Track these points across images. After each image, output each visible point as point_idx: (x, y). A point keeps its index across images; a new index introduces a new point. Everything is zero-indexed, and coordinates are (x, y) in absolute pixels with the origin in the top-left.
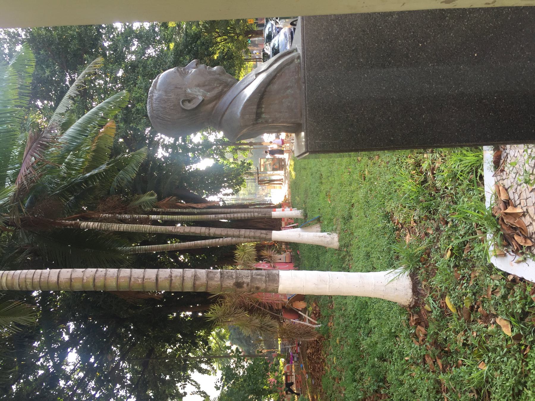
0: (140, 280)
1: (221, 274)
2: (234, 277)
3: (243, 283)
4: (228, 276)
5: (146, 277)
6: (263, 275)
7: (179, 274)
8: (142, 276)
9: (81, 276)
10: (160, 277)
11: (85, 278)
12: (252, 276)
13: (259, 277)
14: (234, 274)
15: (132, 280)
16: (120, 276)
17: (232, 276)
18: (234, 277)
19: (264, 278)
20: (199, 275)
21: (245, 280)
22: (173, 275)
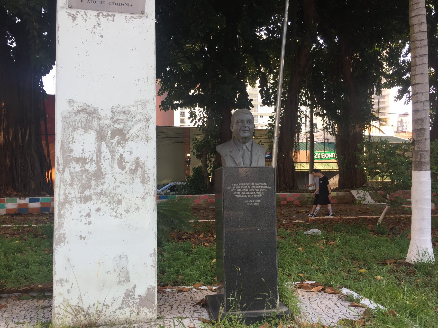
0: (414, 73)
1: (421, 129)
2: (418, 139)
3: (414, 146)
4: (419, 134)
5: (416, 76)
6: (420, 159)
7: (419, 99)
8: (416, 73)
9: (415, 32)
10: (417, 86)
11: (414, 35)
12: (419, 151)
13: (419, 156)
14: (421, 138)
15: (414, 68)
16: (416, 58)
17: (419, 137)
18: (418, 139)
19: (418, 160)
20: (419, 113)
21: (416, 146)
22: (418, 95)
